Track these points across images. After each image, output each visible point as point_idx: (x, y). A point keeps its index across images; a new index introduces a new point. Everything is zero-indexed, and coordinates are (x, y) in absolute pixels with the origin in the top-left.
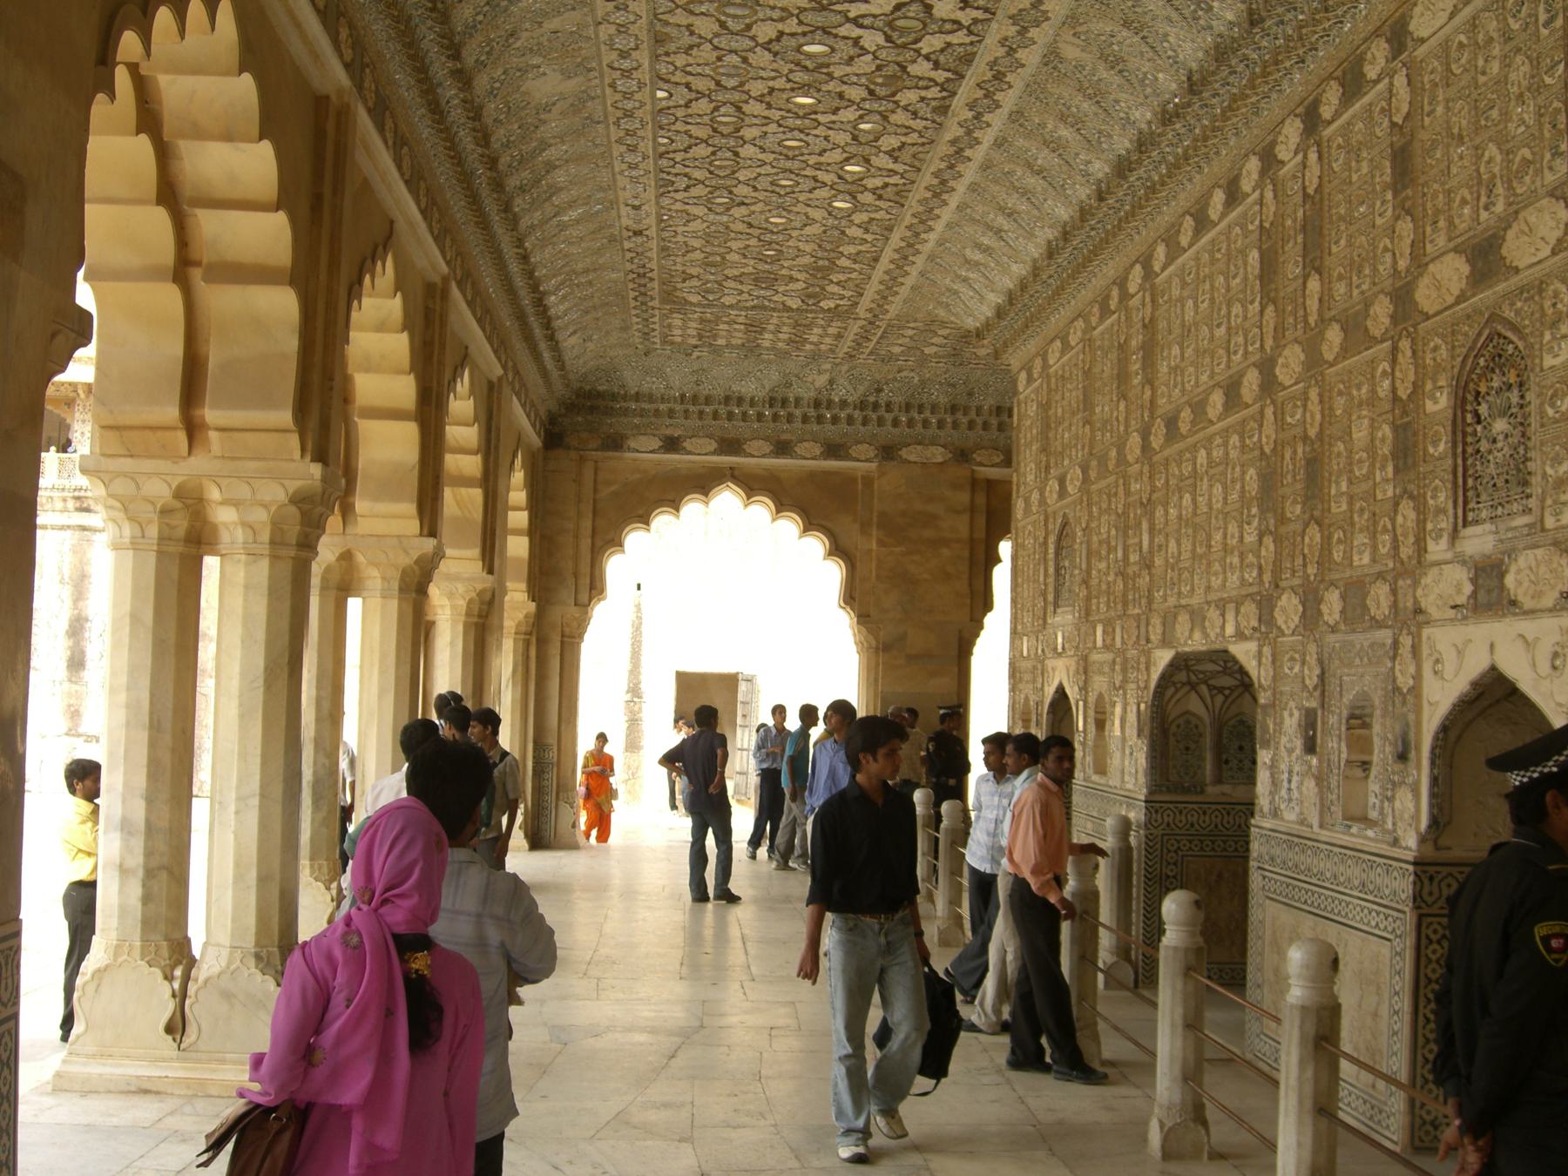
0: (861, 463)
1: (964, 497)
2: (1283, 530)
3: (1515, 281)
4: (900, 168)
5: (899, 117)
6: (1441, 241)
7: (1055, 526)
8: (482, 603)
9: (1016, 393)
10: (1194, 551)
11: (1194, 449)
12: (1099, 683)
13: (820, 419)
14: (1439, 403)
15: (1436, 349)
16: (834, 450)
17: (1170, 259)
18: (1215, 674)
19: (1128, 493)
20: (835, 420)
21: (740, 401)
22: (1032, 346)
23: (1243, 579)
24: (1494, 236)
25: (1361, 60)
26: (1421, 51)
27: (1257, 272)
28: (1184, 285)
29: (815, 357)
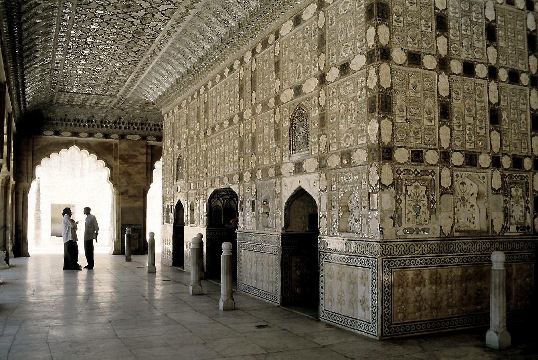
0: (114, 140)
1: (145, 150)
2: (245, 156)
3: (305, 96)
4: (137, 56)
5: (140, 43)
6: (287, 85)
7: (177, 157)
8: (6, 180)
9: (164, 120)
10: (220, 162)
11: (220, 136)
12: (191, 199)
13: (102, 127)
14: (286, 124)
15: (286, 111)
16: (106, 136)
17: (213, 85)
18: (224, 195)
19: (200, 147)
20: (107, 127)
21: (78, 121)
22: (170, 107)
23: (234, 169)
24: (300, 85)
25: (267, 39)
26: (283, 39)
27: (238, 90)
28: (217, 92)
29: (102, 108)
